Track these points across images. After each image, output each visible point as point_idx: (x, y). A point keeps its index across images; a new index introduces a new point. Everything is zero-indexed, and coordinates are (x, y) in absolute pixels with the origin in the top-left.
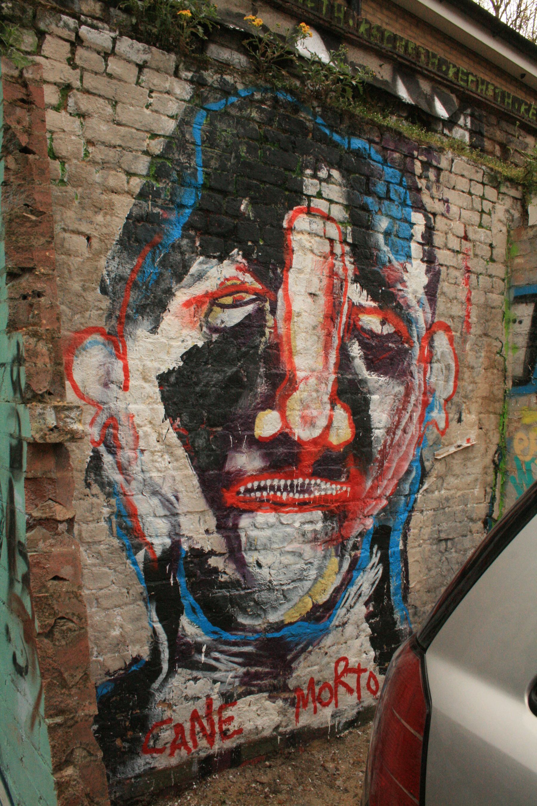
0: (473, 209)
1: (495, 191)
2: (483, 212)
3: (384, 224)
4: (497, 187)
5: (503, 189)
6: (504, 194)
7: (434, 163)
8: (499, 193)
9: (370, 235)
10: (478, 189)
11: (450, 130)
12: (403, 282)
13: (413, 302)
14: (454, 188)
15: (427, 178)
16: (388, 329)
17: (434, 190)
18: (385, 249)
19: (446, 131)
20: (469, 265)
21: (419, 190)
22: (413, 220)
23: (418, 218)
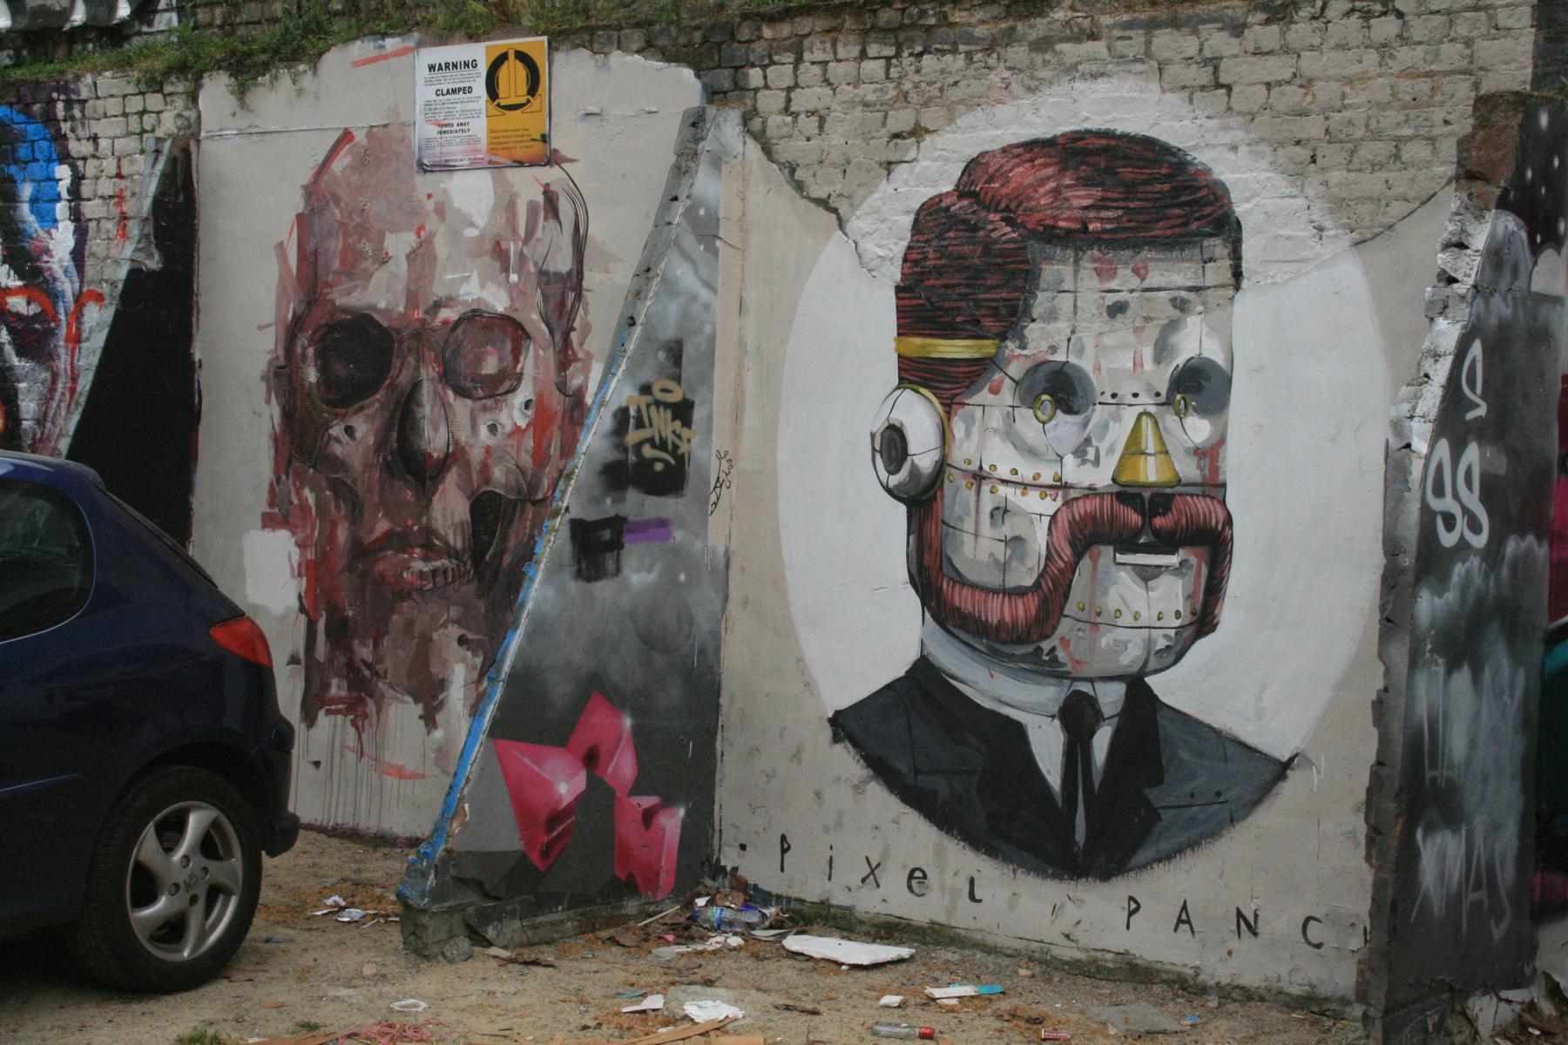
0: (129, 134)
1: (159, 96)
2: (144, 131)
3: (26, 191)
4: (160, 91)
5: (168, 89)
6: (171, 94)
7: (74, 97)
8: (165, 96)
9: (15, 209)
10: (135, 104)
11: (150, 24)
12: (47, 251)
13: (59, 273)
14: (105, 116)
15: (73, 118)
16: (34, 309)
17: (80, 129)
18: (32, 218)
19: (145, 29)
20: (125, 209)
21: (65, 137)
22: (57, 176)
23: (63, 172)
